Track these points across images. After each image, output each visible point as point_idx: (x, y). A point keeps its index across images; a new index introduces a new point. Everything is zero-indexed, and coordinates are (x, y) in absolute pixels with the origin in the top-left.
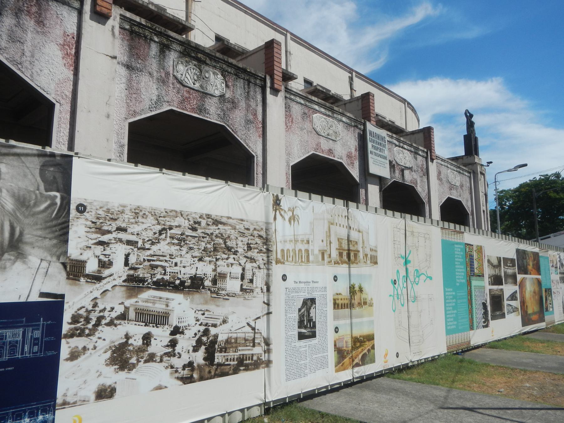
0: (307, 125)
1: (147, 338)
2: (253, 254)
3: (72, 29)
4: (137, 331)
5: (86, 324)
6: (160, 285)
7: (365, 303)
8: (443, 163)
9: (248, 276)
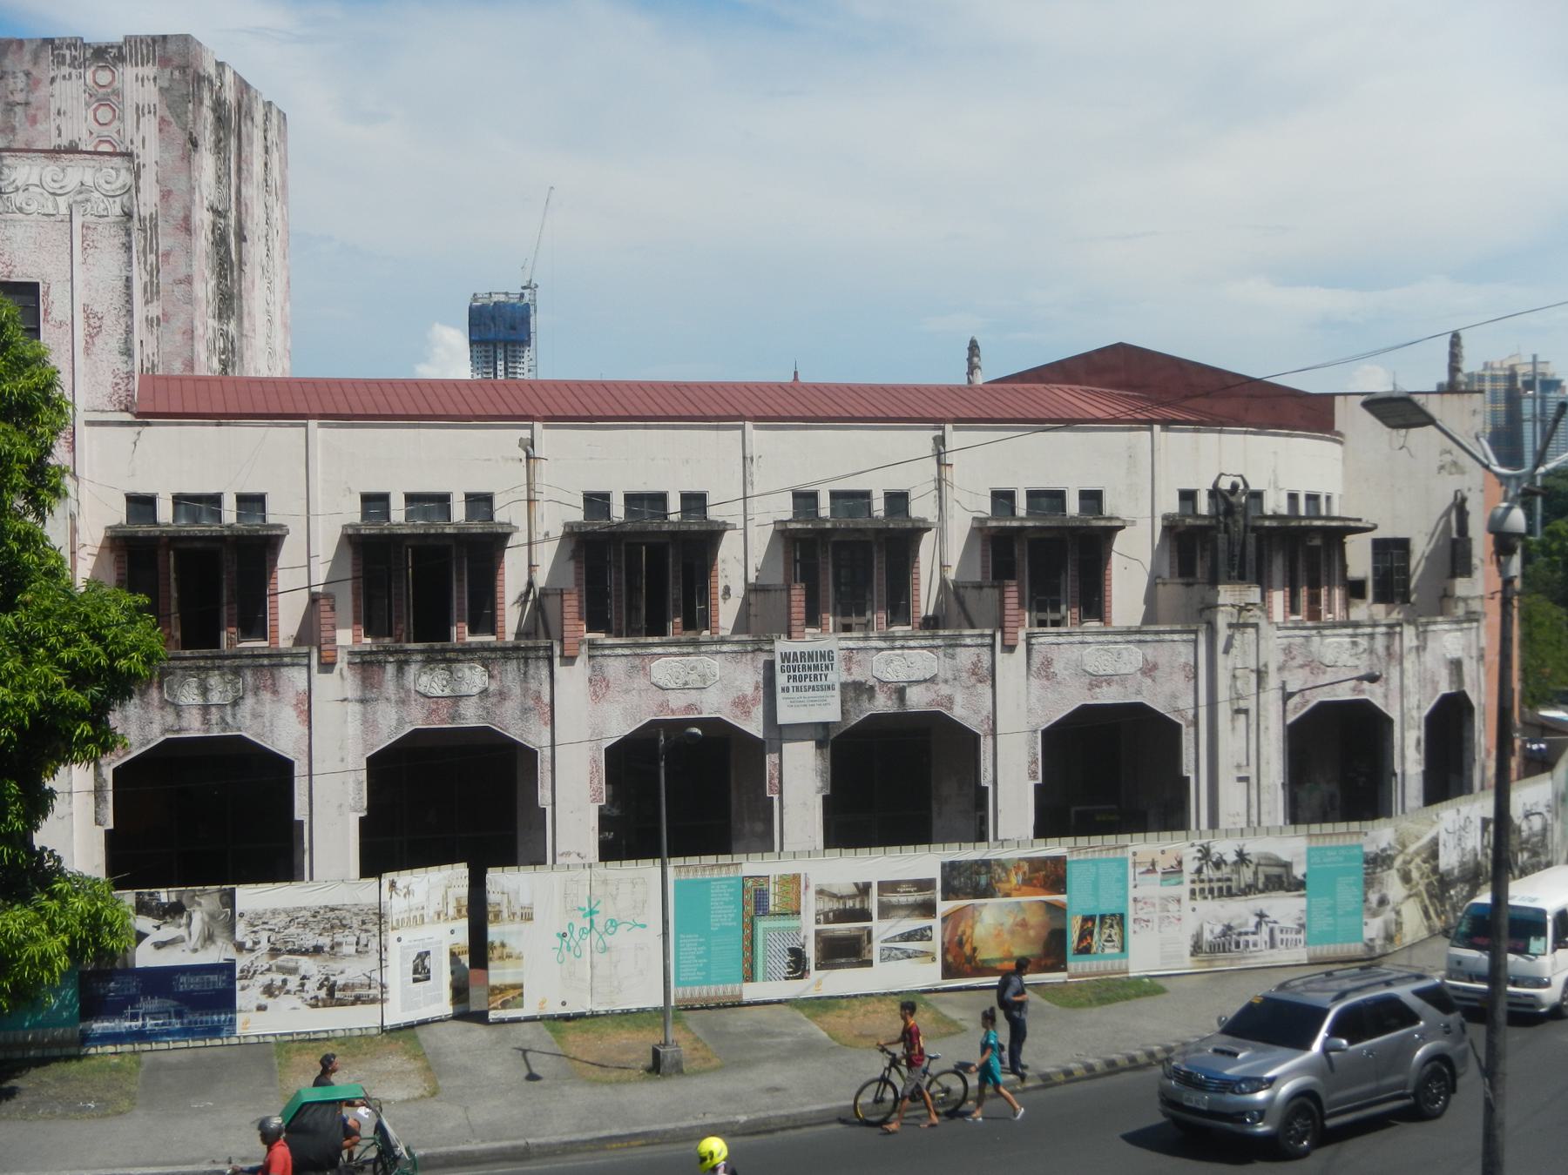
0: (640, 682)
1: (285, 982)
2: (369, 926)
3: (303, 685)
4: (278, 978)
5: (248, 974)
6: (291, 952)
7: (509, 956)
8: (1061, 640)
9: (363, 942)
